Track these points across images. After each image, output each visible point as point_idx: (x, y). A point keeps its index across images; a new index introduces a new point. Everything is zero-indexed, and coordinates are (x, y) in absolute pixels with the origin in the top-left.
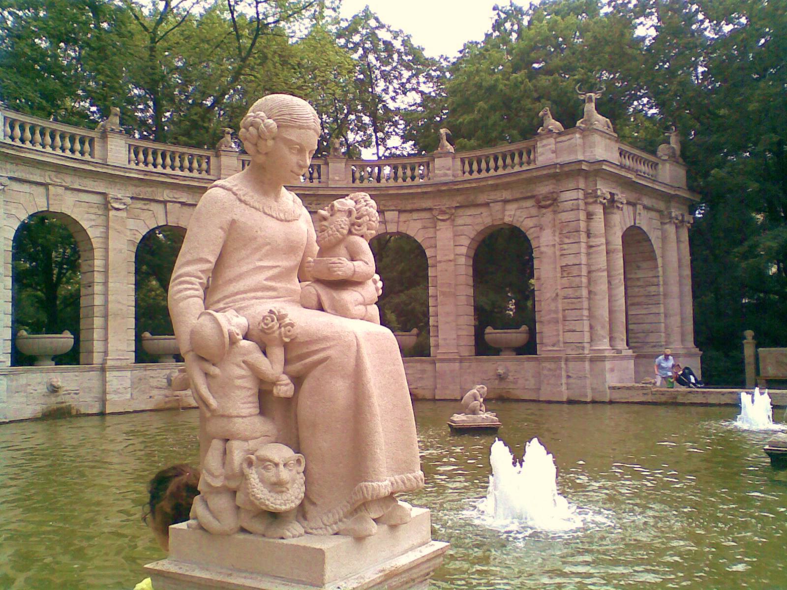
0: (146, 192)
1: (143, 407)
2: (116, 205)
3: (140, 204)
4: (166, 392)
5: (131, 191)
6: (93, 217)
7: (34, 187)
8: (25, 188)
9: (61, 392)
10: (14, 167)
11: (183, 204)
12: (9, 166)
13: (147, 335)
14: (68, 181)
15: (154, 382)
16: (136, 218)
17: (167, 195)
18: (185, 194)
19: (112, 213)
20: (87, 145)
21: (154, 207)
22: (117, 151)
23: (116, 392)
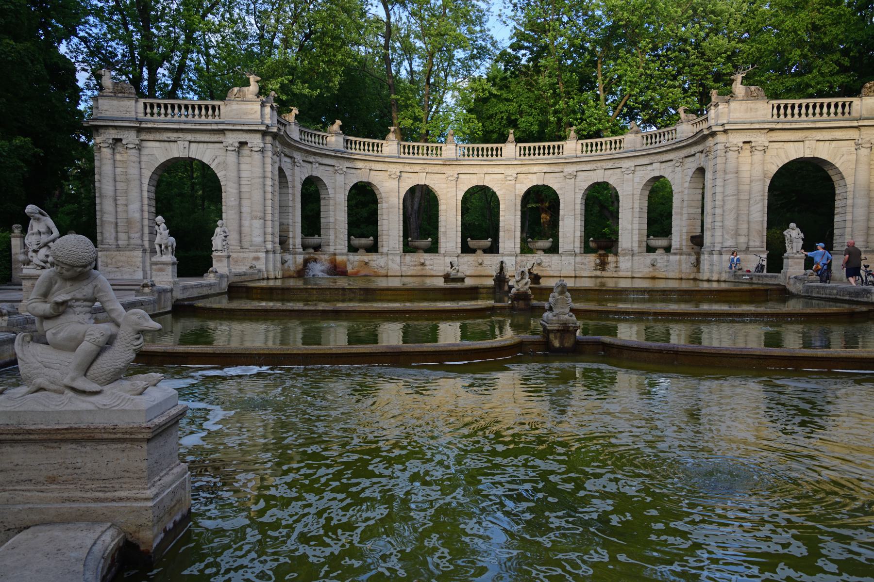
16: (522, 182)
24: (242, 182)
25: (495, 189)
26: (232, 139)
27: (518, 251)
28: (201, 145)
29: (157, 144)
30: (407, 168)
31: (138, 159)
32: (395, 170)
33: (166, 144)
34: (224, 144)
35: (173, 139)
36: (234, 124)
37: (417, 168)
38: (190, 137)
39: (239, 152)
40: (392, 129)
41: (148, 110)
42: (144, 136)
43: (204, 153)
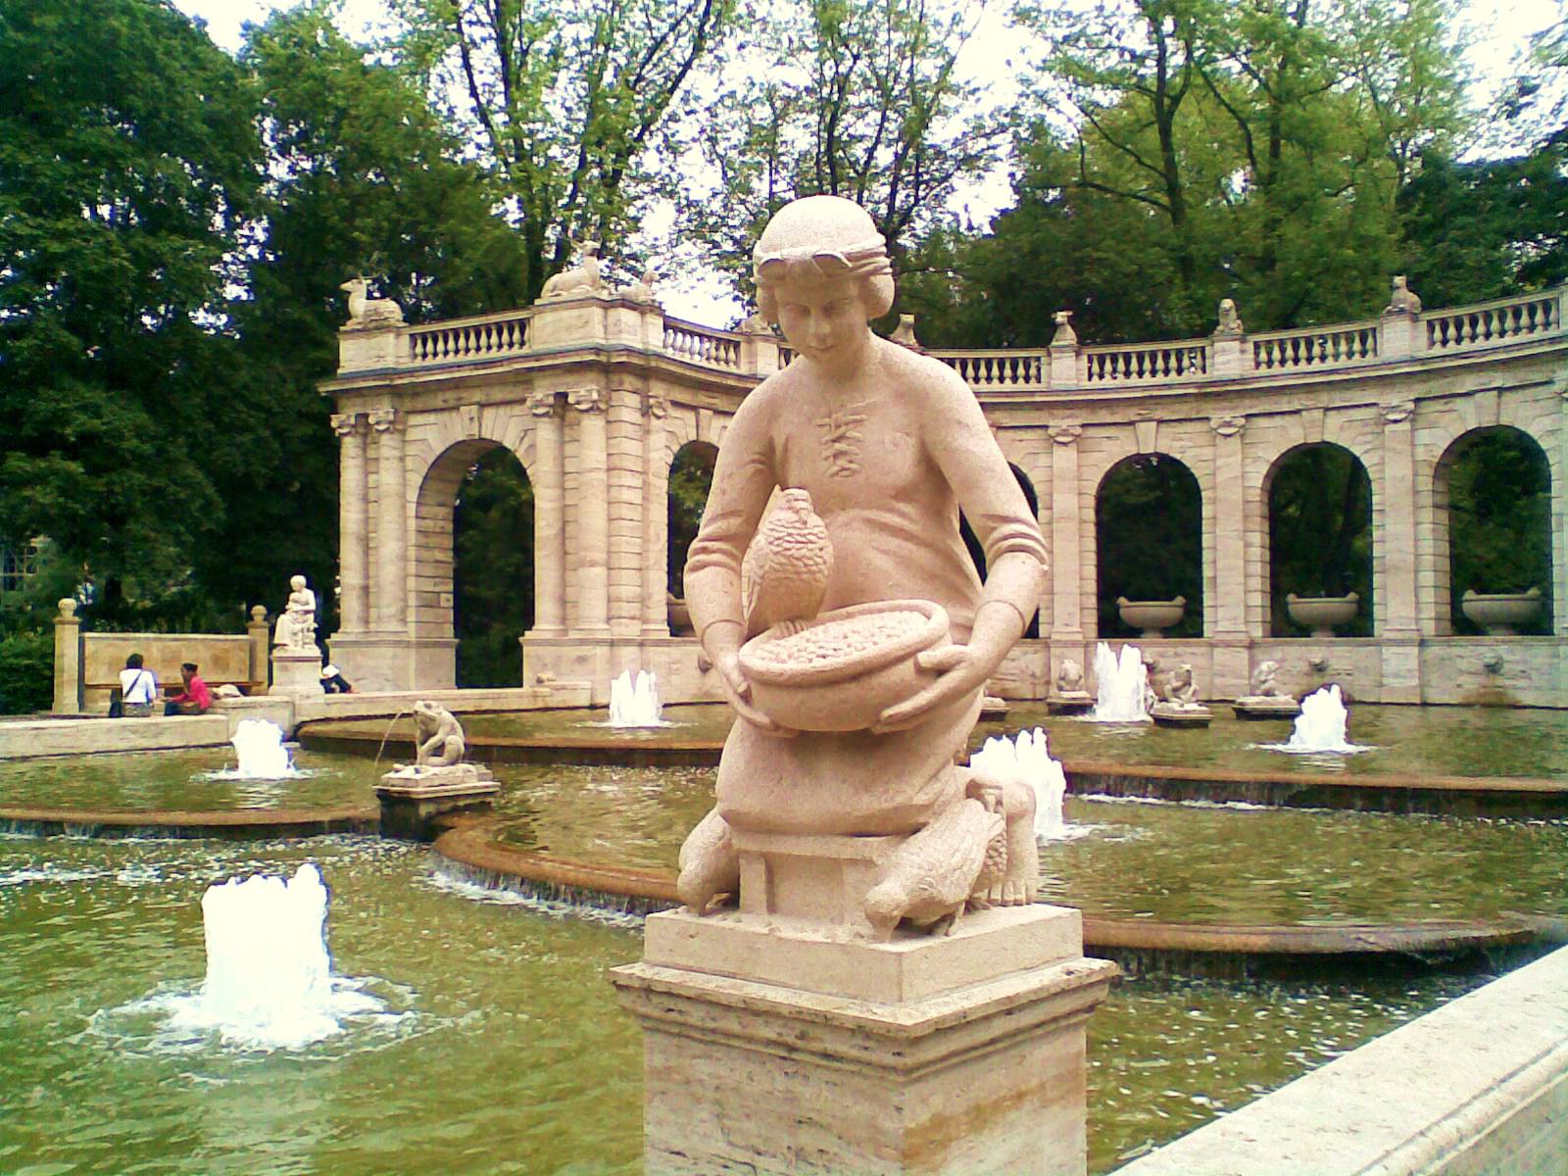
0: (1436, 387)
1: (1446, 699)
2: (1392, 417)
3: (1439, 406)
4: (1481, 680)
5: (1420, 390)
6: (1369, 438)
7: (1288, 418)
8: (1278, 421)
9: (1329, 671)
10: (1254, 402)
11: (1500, 390)
12: (1247, 402)
13: (1469, 595)
14: (1324, 399)
15: (1463, 665)
17: (1469, 383)
18: (1499, 375)
19: (1389, 428)
20: (1370, 340)
21: (1459, 403)
22: (1401, 338)
23: (1396, 676)
24: (569, 484)
25: (1357, 451)
26: (542, 392)
27: (1429, 628)
28: (502, 410)
29: (432, 418)
30: (1104, 416)
31: (397, 453)
32: (1064, 424)
33: (446, 415)
34: (529, 403)
35: (452, 403)
36: (538, 357)
37: (1131, 414)
38: (478, 396)
39: (562, 418)
40: (1061, 317)
41: (419, 349)
42: (408, 404)
43: (503, 428)
